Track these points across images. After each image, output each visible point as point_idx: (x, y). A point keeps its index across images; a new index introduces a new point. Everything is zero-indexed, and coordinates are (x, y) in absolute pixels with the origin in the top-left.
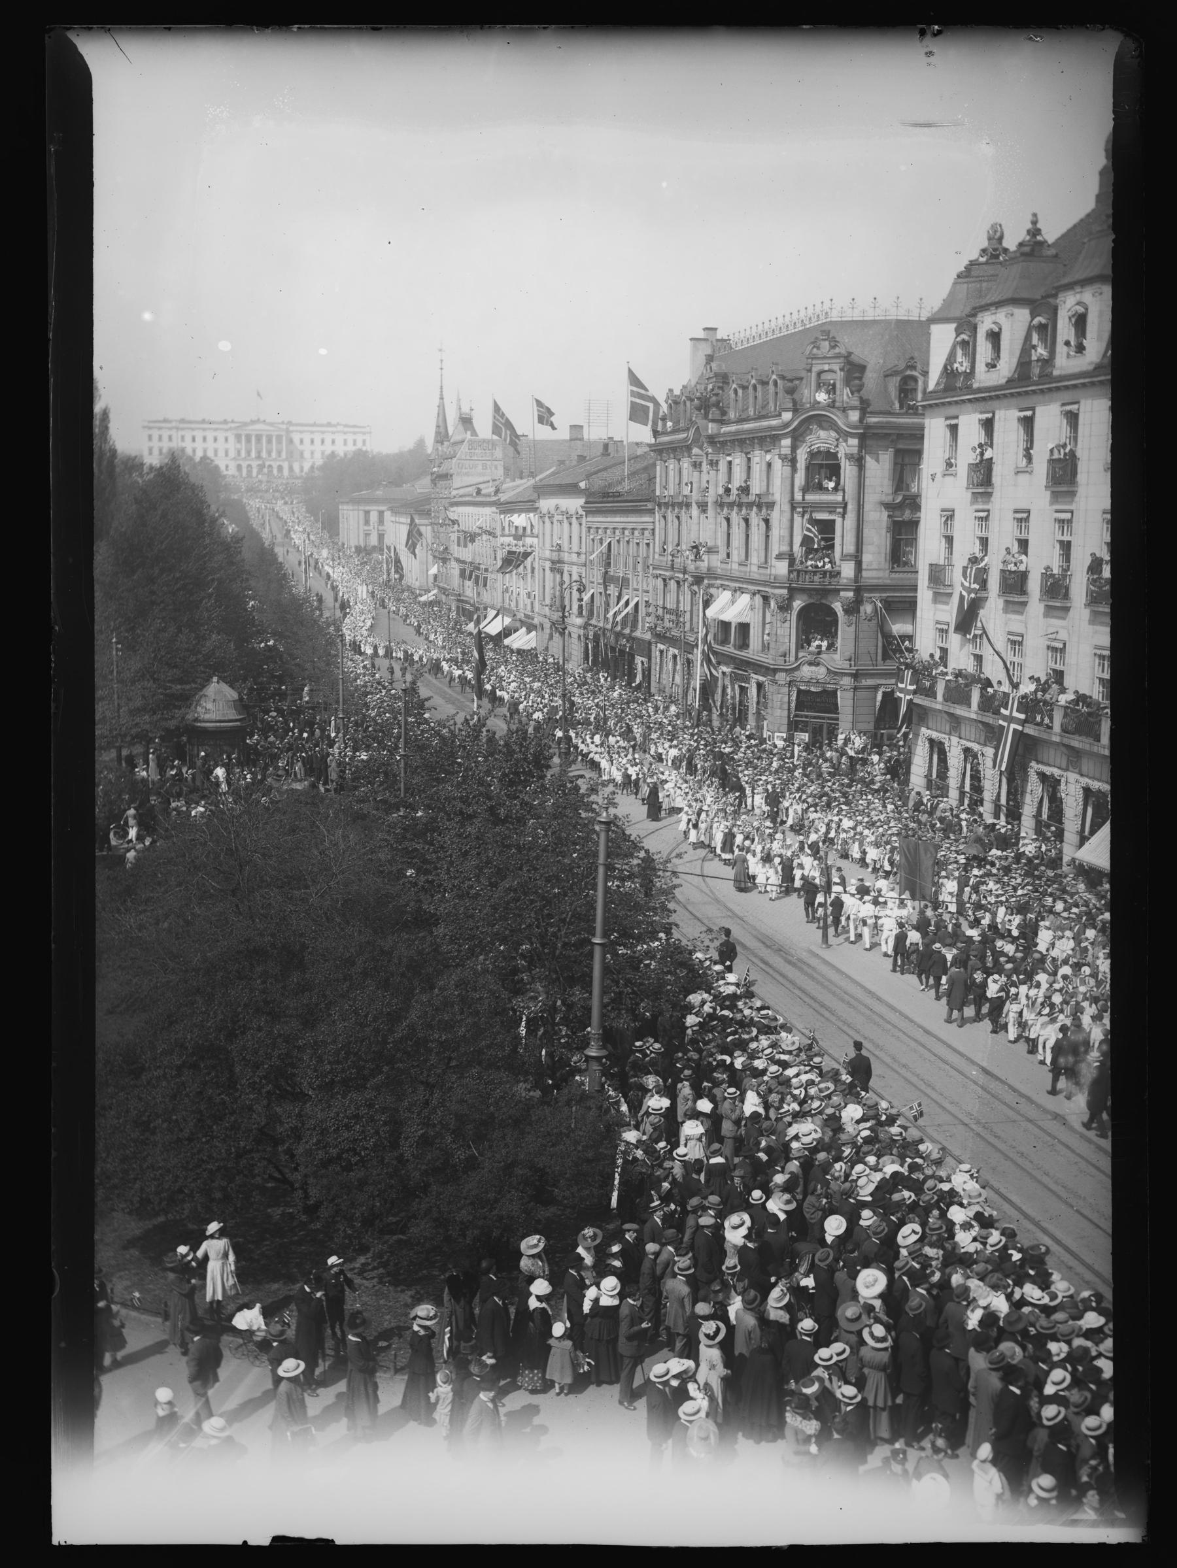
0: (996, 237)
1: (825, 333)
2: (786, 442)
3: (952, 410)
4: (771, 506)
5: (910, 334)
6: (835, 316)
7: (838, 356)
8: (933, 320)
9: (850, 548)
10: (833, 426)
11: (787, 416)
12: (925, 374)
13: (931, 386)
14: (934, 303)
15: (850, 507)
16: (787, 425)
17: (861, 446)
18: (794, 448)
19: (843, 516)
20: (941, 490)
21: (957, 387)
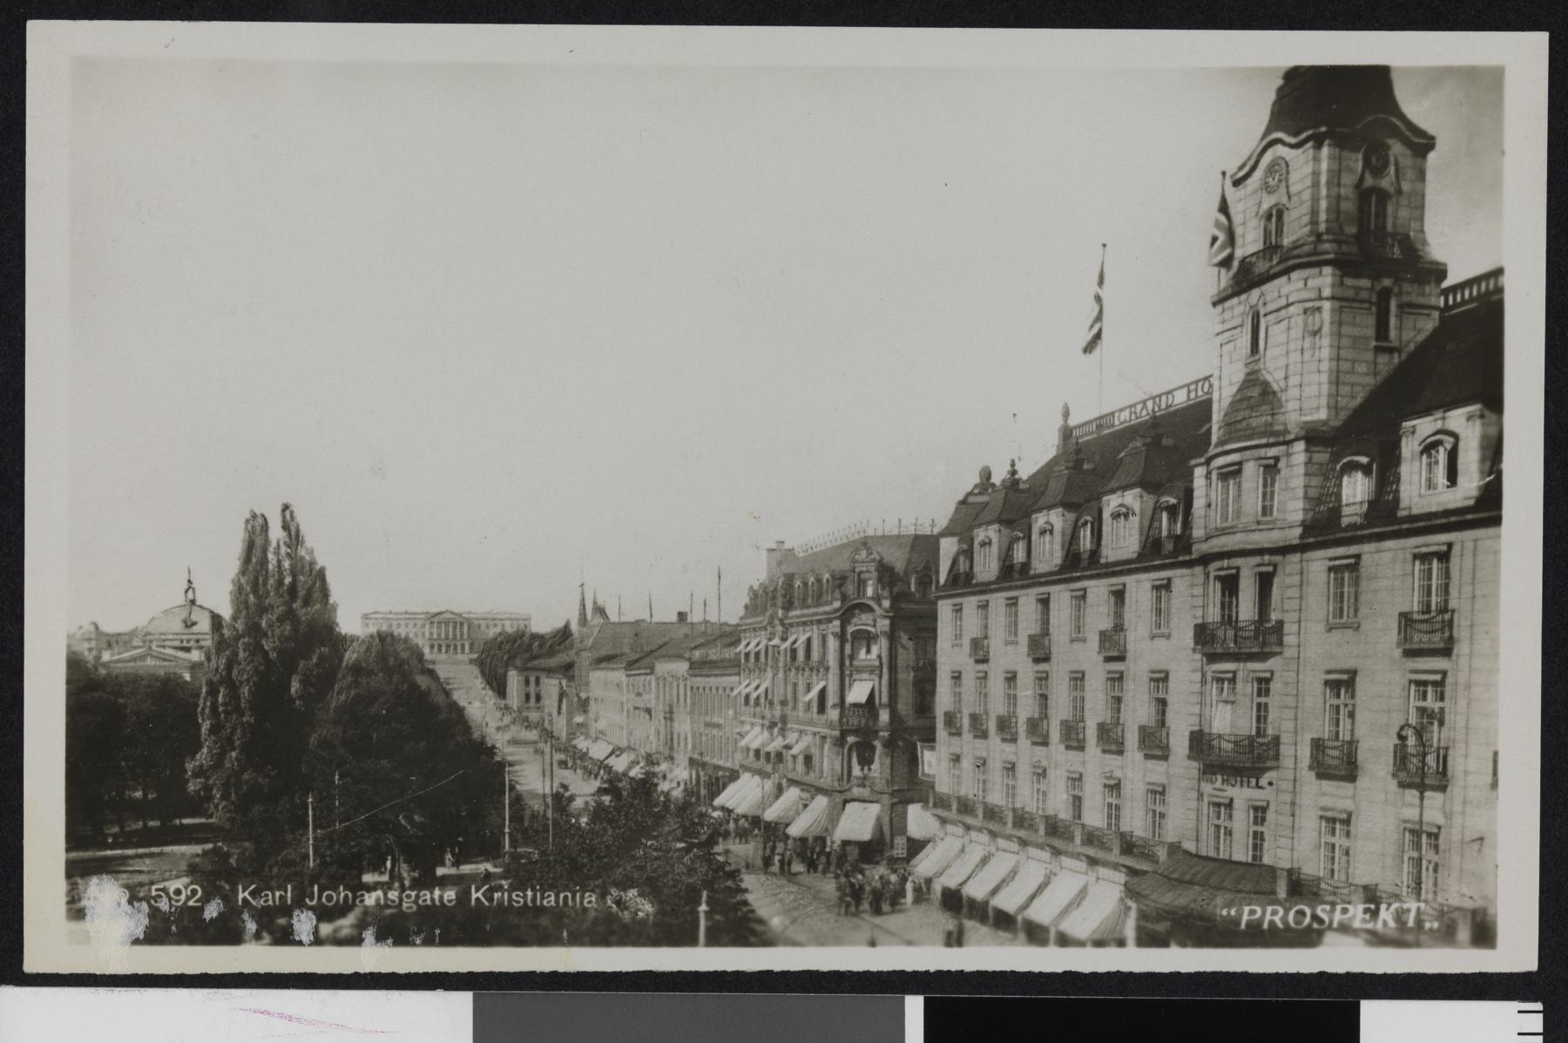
0: (986, 474)
1: (865, 543)
2: (837, 623)
3: (957, 600)
4: (827, 669)
5: (925, 545)
6: (870, 532)
7: (873, 561)
8: (944, 534)
9: (885, 699)
10: (870, 609)
11: (837, 604)
12: (937, 573)
13: (942, 581)
14: (942, 523)
15: (885, 670)
16: (836, 610)
17: (892, 625)
18: (843, 627)
19: (881, 677)
20: (950, 654)
21: (962, 582)
